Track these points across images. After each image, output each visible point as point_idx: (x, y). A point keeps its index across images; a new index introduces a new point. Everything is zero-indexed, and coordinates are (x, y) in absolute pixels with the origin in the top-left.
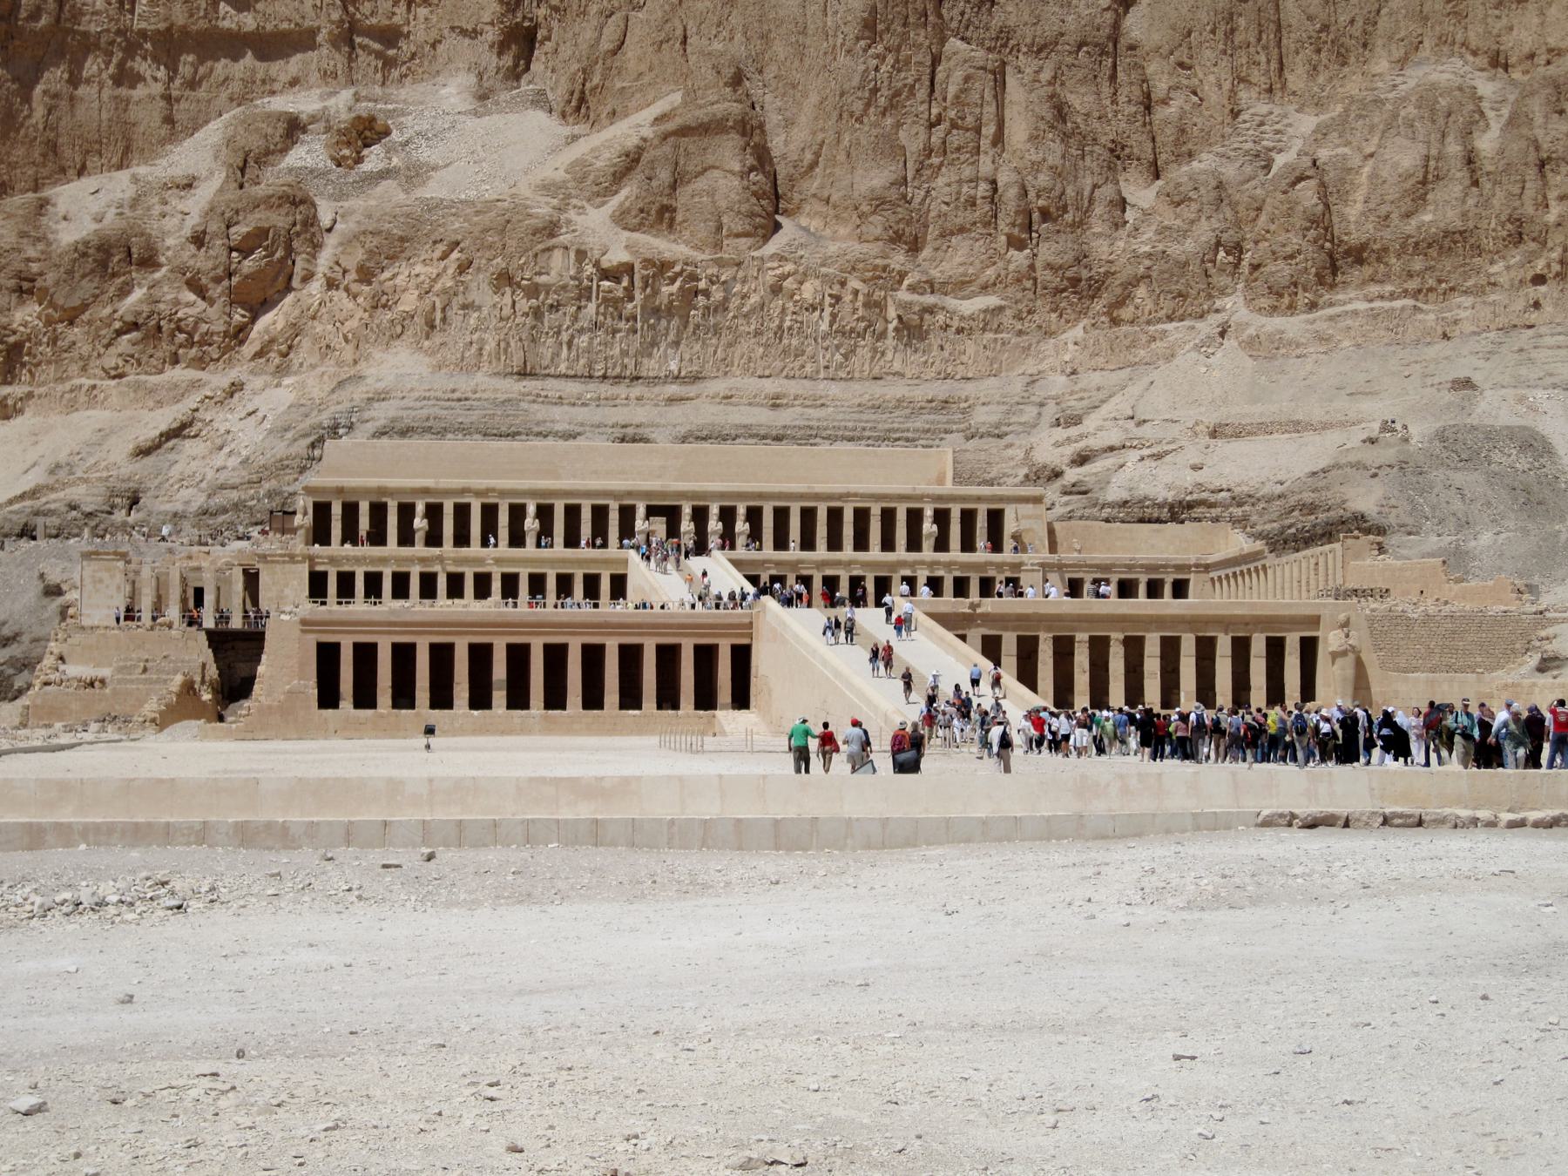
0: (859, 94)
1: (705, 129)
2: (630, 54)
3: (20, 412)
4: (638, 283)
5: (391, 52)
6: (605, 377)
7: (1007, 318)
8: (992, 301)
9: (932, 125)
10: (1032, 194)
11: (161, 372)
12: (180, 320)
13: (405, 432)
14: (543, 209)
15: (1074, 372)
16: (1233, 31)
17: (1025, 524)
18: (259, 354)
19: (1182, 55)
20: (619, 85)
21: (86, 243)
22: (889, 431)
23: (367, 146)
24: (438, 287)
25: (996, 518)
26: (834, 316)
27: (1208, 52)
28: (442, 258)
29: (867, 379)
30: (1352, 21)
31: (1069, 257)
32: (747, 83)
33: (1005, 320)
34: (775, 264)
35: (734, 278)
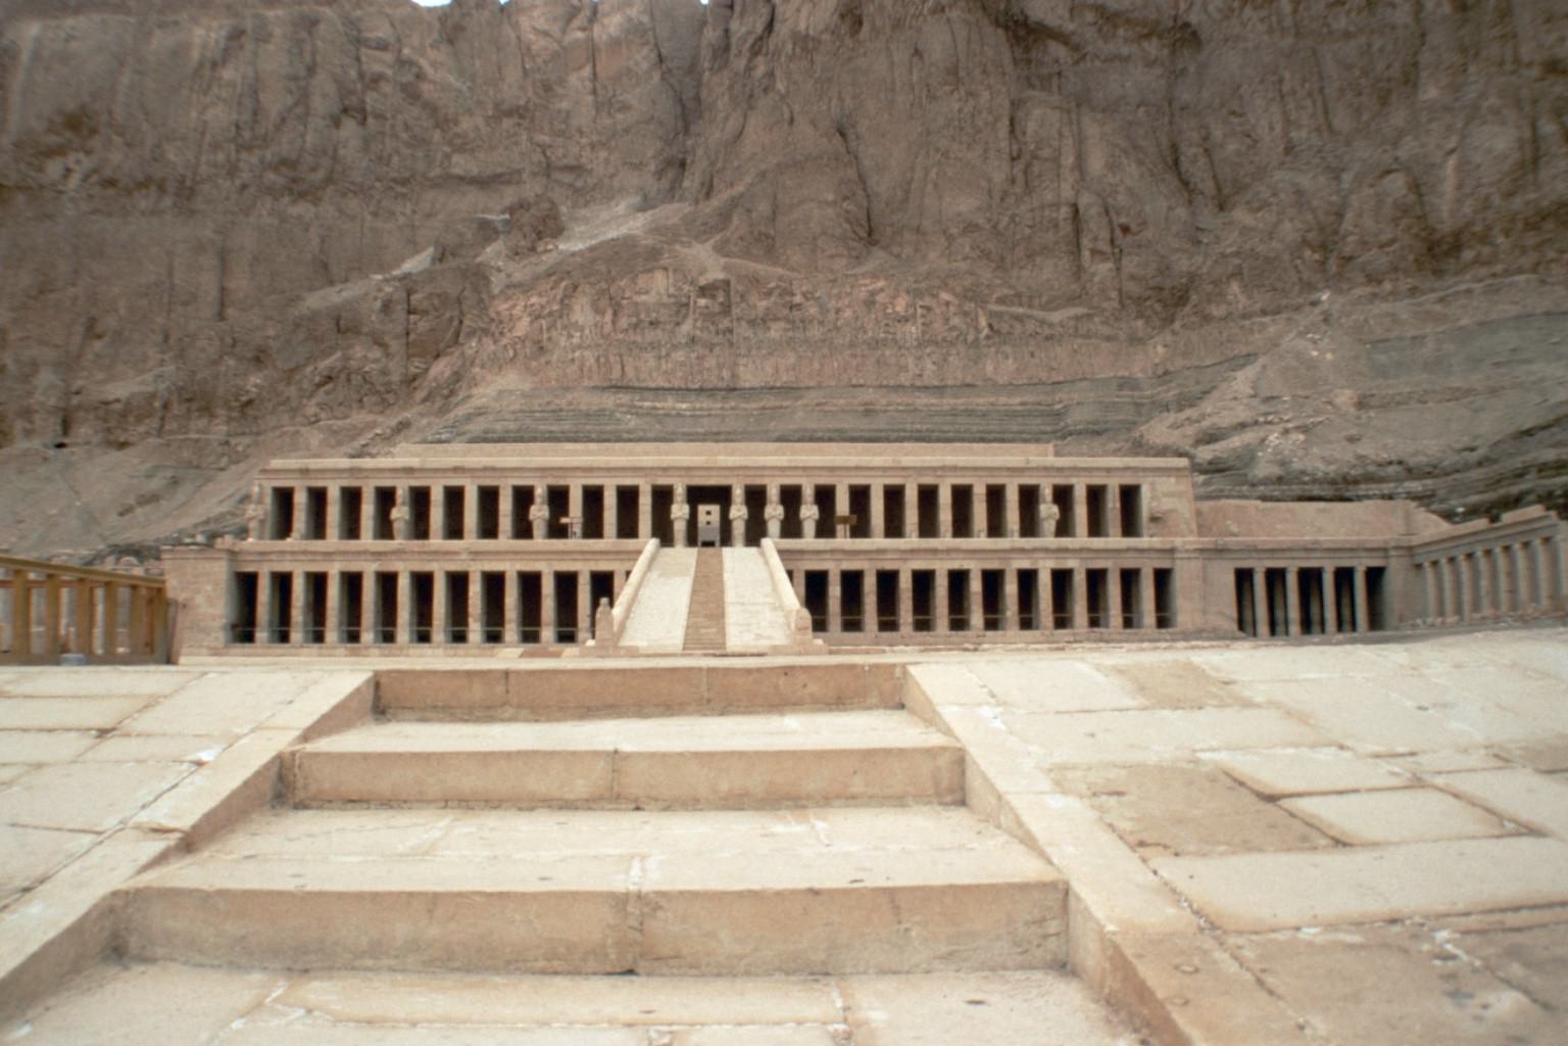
3: (247, 457)
4: (735, 299)
6: (701, 390)
7: (1096, 325)
8: (1080, 311)
9: (1013, 159)
10: (1112, 213)
16: (1281, 81)
17: (1167, 504)
18: (425, 400)
20: (736, 163)
23: (540, 239)
24: (546, 311)
25: (1129, 495)
30: (1389, 66)
33: (1092, 327)
34: (867, 281)
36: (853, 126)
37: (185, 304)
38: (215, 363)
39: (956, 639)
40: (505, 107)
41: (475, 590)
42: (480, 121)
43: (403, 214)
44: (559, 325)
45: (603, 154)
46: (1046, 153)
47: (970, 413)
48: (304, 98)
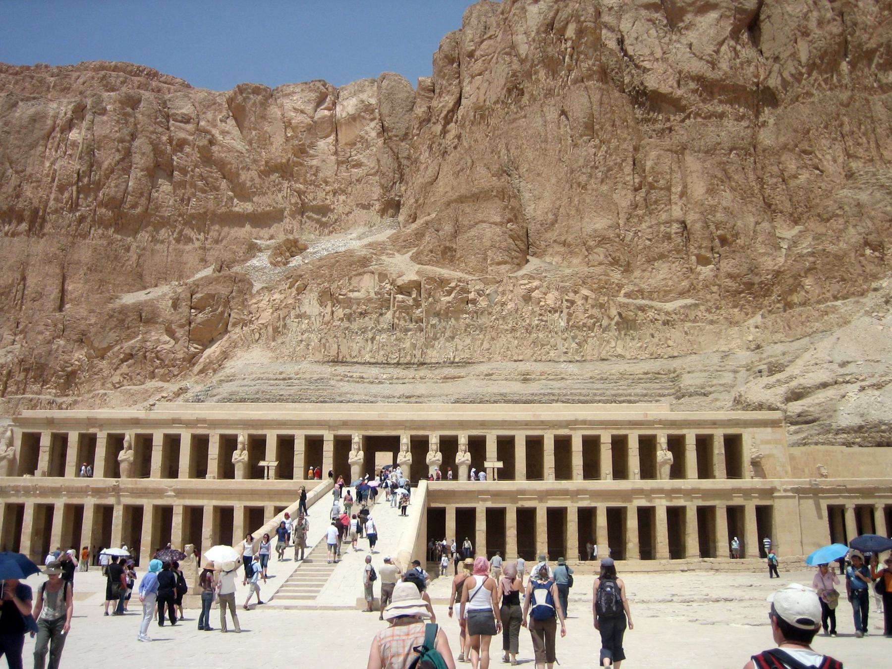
0: (584, 170)
1: (476, 198)
2: (441, 183)
5: (324, 219)
6: (398, 364)
7: (701, 312)
8: (689, 301)
9: (636, 190)
11: (143, 383)
12: (158, 351)
13: (236, 401)
14: (364, 252)
15: (758, 347)
16: (841, 125)
17: (764, 450)
19: (805, 146)
21: (114, 310)
22: (615, 395)
25: (733, 444)
26: (570, 315)
27: (824, 141)
28: (290, 288)
29: (597, 361)
31: (744, 268)
32: (488, 103)
33: (699, 314)
35: (496, 292)
36: (517, 169)
37: (34, 300)
38: (50, 342)
39: (586, 567)
40: (272, 163)
41: (177, 521)
42: (254, 174)
43: (198, 239)
44: (293, 313)
45: (342, 198)
46: (662, 183)
47: (603, 380)
48: (128, 153)
